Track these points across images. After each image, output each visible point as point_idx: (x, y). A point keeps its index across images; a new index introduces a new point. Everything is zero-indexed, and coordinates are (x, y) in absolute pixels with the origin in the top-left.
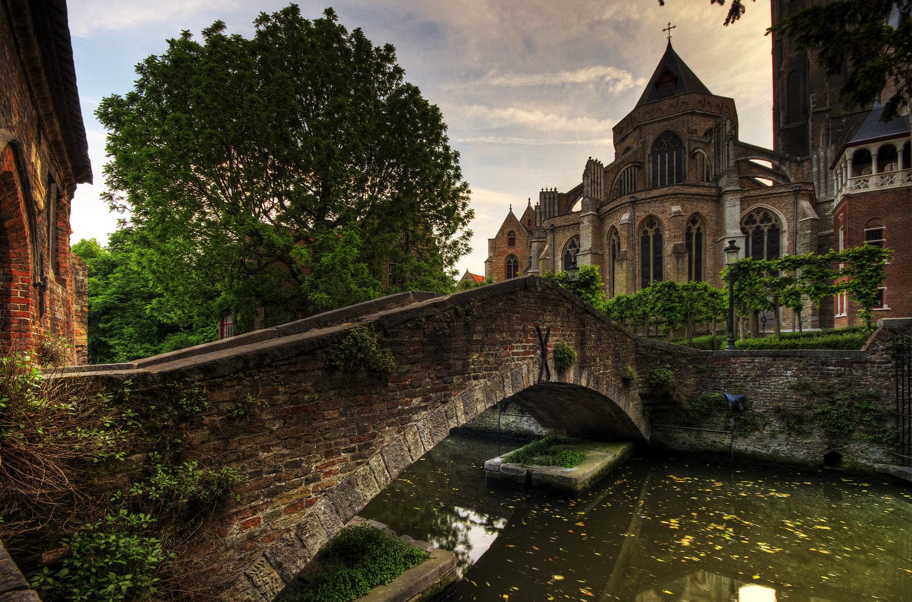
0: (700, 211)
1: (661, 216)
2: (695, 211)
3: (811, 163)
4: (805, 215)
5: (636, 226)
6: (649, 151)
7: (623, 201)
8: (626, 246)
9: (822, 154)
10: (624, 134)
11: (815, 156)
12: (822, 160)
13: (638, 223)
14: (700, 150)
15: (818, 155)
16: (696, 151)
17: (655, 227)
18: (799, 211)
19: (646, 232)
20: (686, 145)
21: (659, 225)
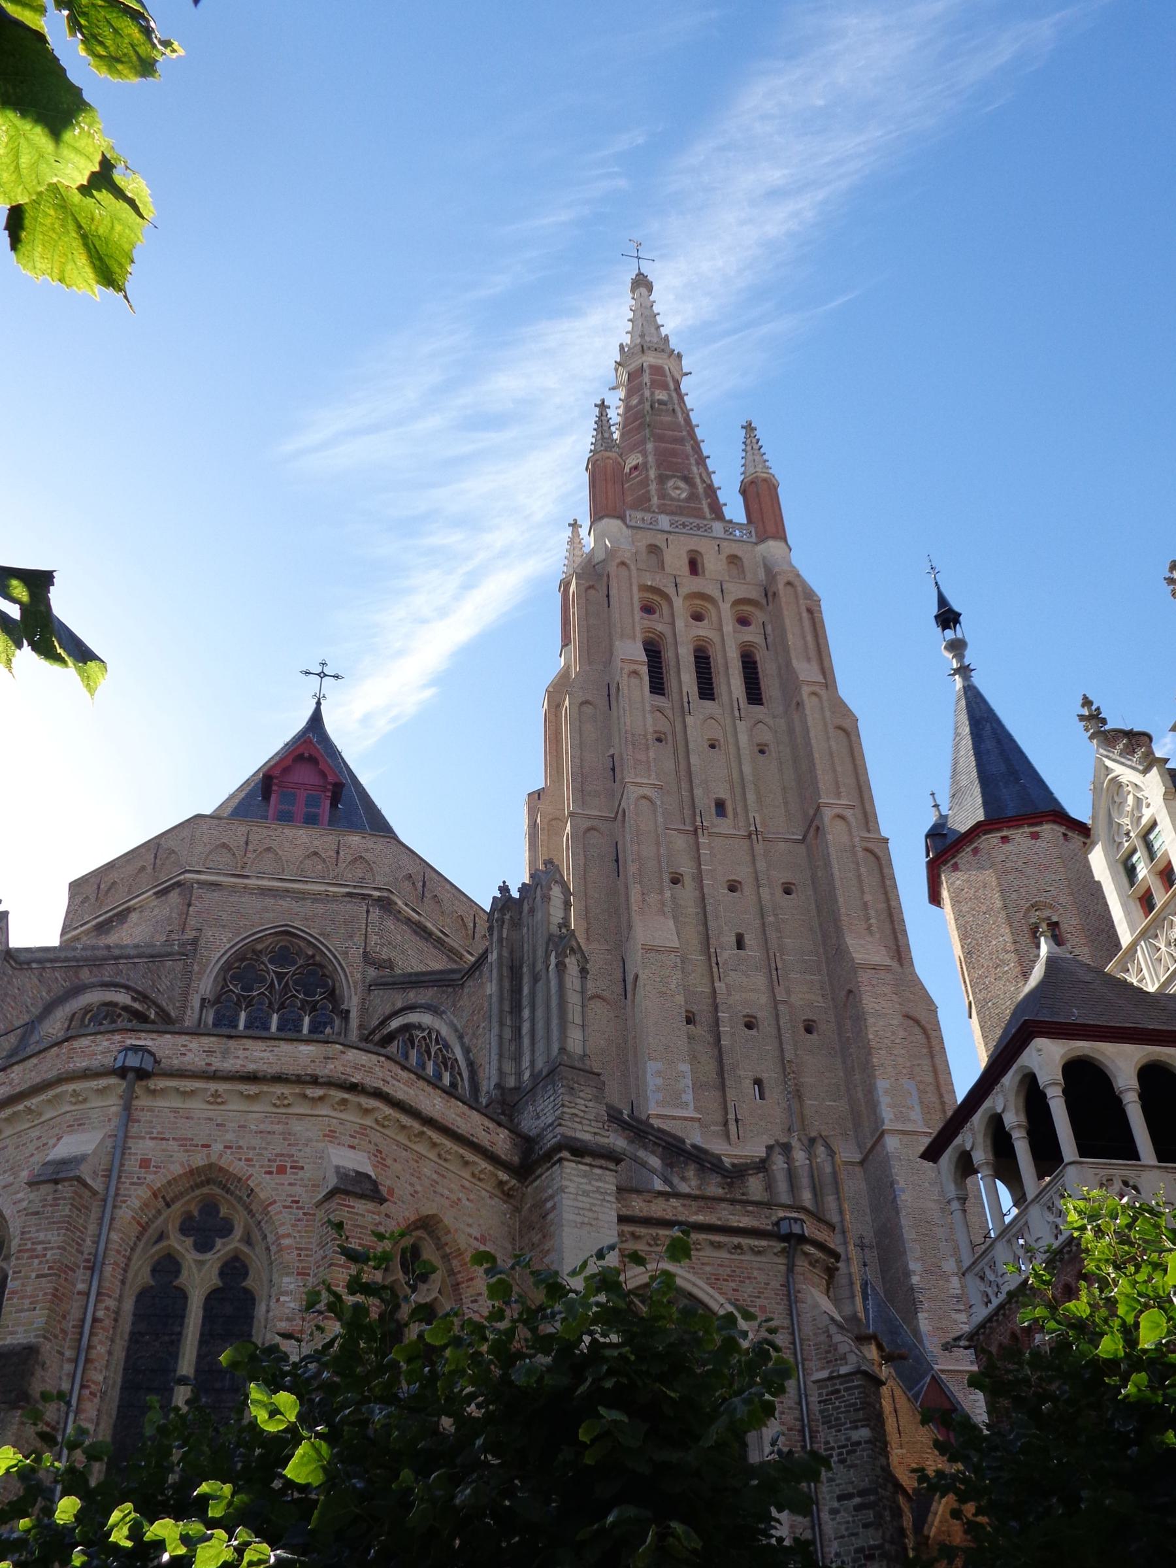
0: (448, 1220)
1: (266, 1186)
2: (428, 1209)
3: (769, 1187)
4: (831, 1355)
5: (125, 1214)
6: (206, 985)
7: (81, 1063)
8: (39, 1318)
9: (800, 1156)
10: (114, 903)
11: (779, 1163)
12: (805, 1181)
13: (135, 1198)
14: (413, 1018)
15: (789, 1160)
16: (395, 1024)
17: (224, 1248)
18: (808, 1330)
19: (168, 1266)
20: (353, 1003)
21: (248, 1240)
